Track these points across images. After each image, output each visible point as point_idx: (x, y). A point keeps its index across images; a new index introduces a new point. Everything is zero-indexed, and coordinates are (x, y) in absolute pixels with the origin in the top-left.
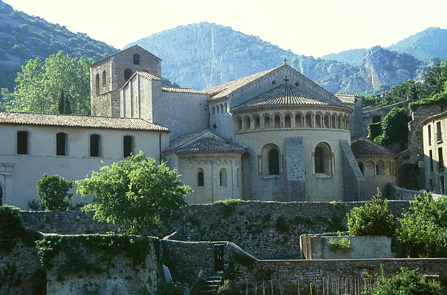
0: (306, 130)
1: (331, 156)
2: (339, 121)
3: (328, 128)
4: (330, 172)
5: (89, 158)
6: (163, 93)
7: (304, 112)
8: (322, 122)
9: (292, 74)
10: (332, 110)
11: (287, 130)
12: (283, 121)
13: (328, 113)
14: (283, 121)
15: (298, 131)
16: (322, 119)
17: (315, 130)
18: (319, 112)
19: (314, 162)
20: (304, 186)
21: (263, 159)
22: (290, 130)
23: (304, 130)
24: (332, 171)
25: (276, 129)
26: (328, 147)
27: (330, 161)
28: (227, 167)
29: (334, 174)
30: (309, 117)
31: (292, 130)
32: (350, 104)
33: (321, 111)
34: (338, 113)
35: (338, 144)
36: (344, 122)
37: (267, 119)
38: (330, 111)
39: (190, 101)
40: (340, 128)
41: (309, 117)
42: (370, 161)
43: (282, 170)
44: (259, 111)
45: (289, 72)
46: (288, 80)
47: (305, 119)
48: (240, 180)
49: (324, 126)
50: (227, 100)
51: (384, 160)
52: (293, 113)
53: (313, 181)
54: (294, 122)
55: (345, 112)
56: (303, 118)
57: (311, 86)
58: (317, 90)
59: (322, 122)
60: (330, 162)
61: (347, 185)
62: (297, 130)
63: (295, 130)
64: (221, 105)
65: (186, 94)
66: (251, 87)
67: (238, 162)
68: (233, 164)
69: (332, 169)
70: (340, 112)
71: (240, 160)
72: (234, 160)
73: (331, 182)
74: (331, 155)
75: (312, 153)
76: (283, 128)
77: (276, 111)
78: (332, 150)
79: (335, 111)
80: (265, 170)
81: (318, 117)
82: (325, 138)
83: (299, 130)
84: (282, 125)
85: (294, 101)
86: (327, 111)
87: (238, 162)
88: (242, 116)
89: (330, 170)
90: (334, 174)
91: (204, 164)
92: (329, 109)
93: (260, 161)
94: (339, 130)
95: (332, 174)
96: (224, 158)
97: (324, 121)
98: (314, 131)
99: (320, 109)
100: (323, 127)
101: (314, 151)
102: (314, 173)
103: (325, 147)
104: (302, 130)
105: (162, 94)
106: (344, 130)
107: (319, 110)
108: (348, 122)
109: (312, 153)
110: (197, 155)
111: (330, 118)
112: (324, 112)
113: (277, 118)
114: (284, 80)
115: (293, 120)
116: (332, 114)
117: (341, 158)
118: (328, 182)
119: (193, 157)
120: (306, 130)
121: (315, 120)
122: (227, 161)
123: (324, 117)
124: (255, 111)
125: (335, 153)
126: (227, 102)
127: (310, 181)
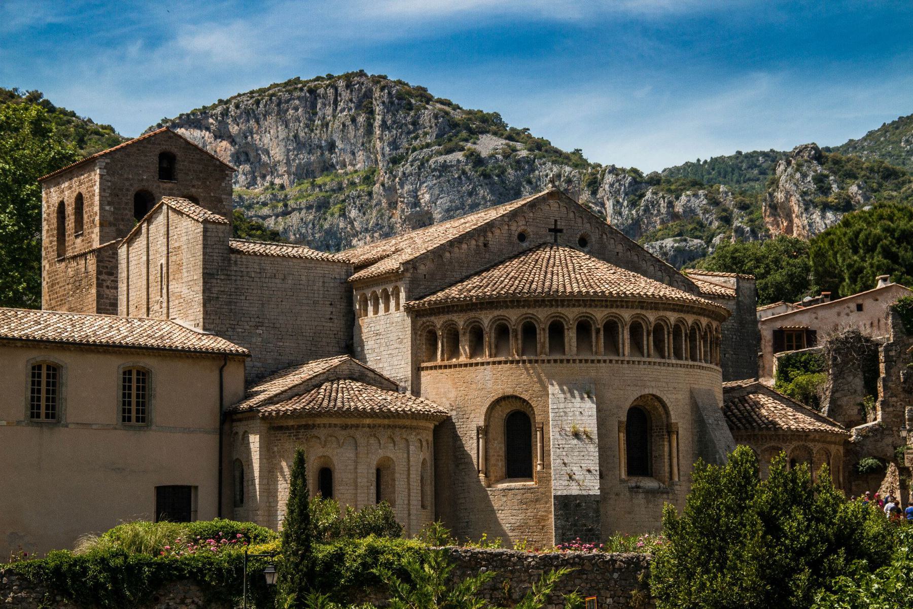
0: (605, 361)
1: (670, 433)
2: (692, 338)
3: (663, 357)
4: (667, 475)
5: (28, 425)
6: (233, 256)
7: (600, 315)
8: (648, 342)
9: (571, 215)
10: (674, 310)
11: (555, 361)
12: (543, 337)
13: (664, 320)
14: (543, 337)
15: (583, 365)
16: (648, 335)
17: (628, 362)
18: (638, 316)
19: (623, 446)
20: (597, 511)
21: (490, 436)
22: (562, 361)
23: (599, 361)
24: (671, 472)
25: (525, 358)
26: (661, 409)
27: (666, 443)
28: (395, 453)
29: (676, 479)
30: (611, 328)
31: (568, 361)
32: (722, 297)
33: (644, 312)
34: (690, 319)
35: (687, 401)
36: (705, 342)
37: (503, 332)
39: (303, 278)
40: (693, 358)
41: (611, 328)
43: (539, 468)
44: (481, 309)
45: (564, 210)
46: (561, 231)
47: (602, 332)
48: (429, 490)
49: (652, 352)
50: (401, 279)
51: (811, 445)
52: (571, 316)
54: (574, 340)
55: (708, 316)
56: (598, 331)
57: (620, 247)
58: (636, 258)
59: (648, 342)
62: (581, 361)
63: (574, 361)
64: (385, 291)
65: (294, 260)
66: (464, 246)
67: (424, 444)
68: (412, 448)
69: (671, 466)
70: (695, 317)
71: (431, 438)
72: (413, 438)
74: (670, 430)
75: (620, 422)
76: (544, 357)
77: (526, 310)
78: (673, 417)
79: (682, 315)
80: (495, 465)
81: (636, 330)
82: (653, 384)
83: (586, 361)
84: (543, 346)
85: (575, 285)
86: (661, 313)
87: (424, 444)
88: (439, 322)
89: (667, 469)
90: (676, 479)
91: (335, 445)
92: (665, 309)
94: (691, 363)
95: (671, 478)
96: (389, 432)
97: (651, 338)
98: (625, 365)
99: (642, 308)
100: (649, 356)
101: (624, 418)
102: (623, 476)
103: (655, 408)
104: (593, 361)
105: (230, 260)
106: (704, 365)
108: (715, 342)
109: (620, 422)
110: (318, 421)
111: (669, 333)
112: (652, 317)
113: (529, 331)
114: (550, 230)
115: (571, 337)
116: (673, 323)
117: (696, 438)
119: (307, 427)
120: (605, 361)
121: (627, 335)
122: (397, 439)
123: (651, 329)
124: (471, 310)
125: (680, 424)
126: (399, 284)
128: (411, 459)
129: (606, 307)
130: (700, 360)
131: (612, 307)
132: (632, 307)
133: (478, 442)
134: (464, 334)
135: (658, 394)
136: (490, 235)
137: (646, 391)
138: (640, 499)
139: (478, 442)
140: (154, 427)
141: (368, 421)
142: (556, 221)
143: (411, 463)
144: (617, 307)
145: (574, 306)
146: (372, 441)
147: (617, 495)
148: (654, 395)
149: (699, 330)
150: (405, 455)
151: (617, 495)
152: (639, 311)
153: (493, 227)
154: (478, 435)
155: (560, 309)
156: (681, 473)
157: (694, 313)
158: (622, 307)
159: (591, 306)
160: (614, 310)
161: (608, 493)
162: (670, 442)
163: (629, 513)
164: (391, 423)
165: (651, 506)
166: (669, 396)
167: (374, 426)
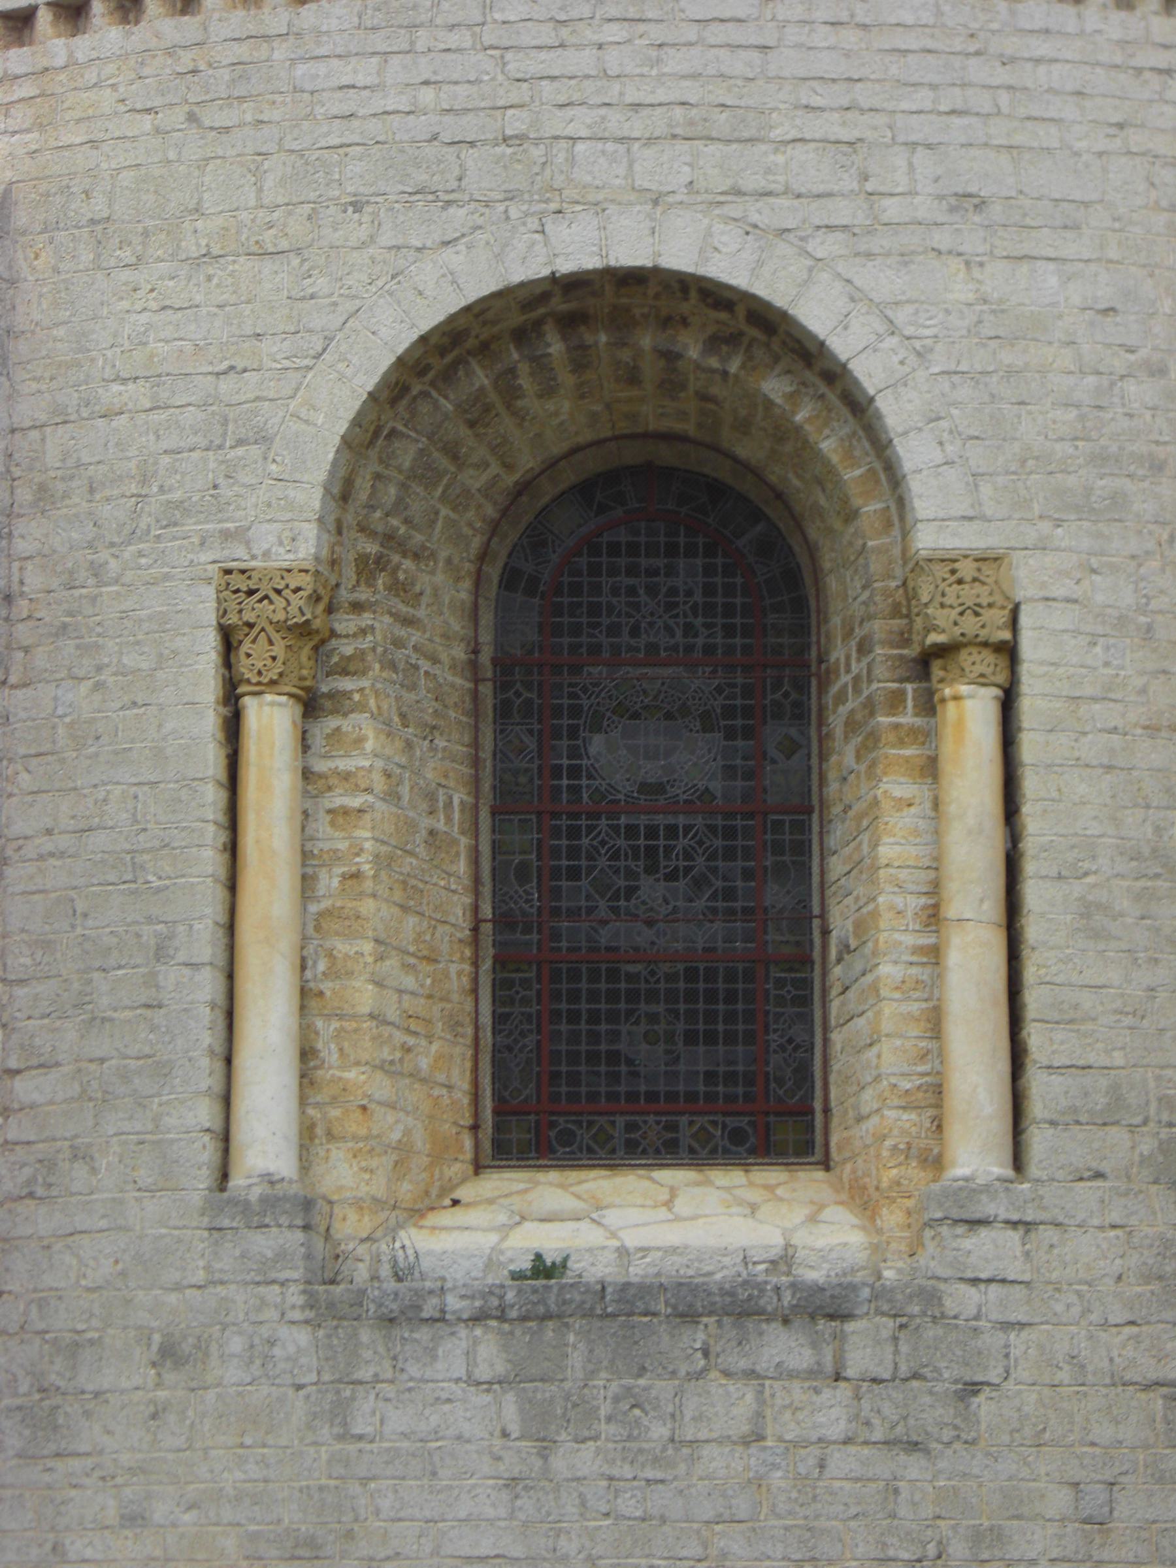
1: (928, 663)
24: (935, 1094)
29: (975, 1154)
60: (896, 846)
69: (935, 1023)
73: (831, 1412)
75: (239, 585)
82: (667, 168)
109: (239, 585)
118: (727, 1405)
125: (1027, 578)
135: (732, 265)
137: (577, 249)
138: (456, 1395)
147: (169, 1354)
156: (1042, 1089)
161: (73, 1349)
162: (931, 769)
165: (578, 1459)
166: (882, 280)
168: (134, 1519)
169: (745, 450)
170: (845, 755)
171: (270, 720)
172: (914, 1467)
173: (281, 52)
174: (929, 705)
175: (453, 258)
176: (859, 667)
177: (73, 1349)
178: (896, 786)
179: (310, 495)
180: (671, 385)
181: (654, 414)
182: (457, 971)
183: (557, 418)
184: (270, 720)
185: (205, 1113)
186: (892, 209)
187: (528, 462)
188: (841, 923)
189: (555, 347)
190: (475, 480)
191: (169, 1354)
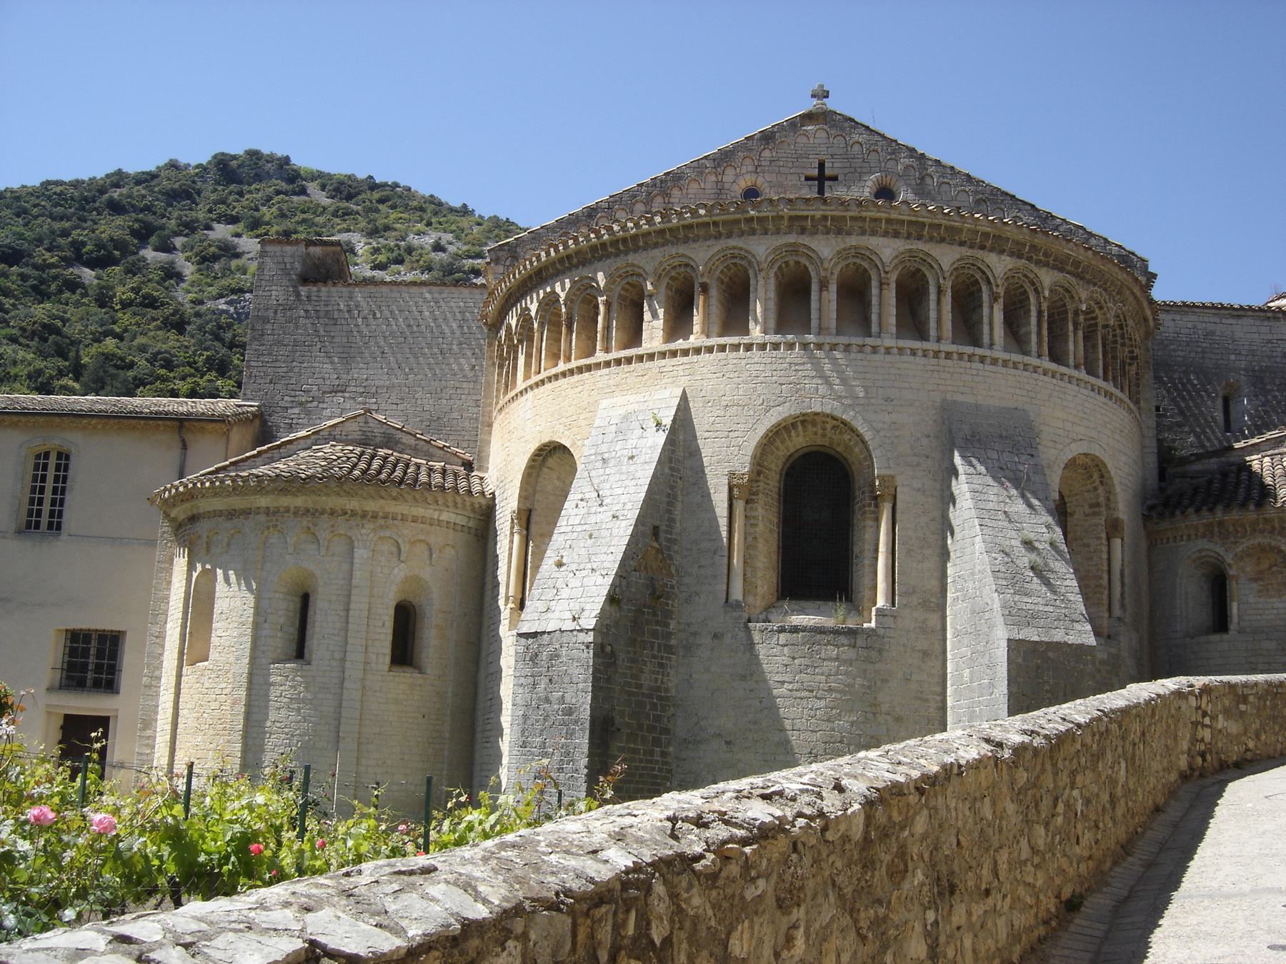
6: (304, 290)
18: (794, 249)
33: (804, 240)
38: (874, 242)
42: (1263, 549)
53: (728, 640)
56: (705, 288)
60: (868, 536)
61: (966, 673)
75: (732, 475)
86: (853, 241)
93: (516, 538)
96: (305, 522)
99: (803, 231)
105: (298, 295)
107: (791, 239)
109: (732, 475)
122: (324, 535)
125: (899, 481)
127: (706, 640)
128: (357, 574)
129: (718, 236)
130: (991, 345)
131: (729, 236)
132: (778, 232)
133: (512, 542)
134: (520, 341)
136: (676, 192)
139: (512, 542)
140: (64, 536)
141: (263, 502)
142: (822, 165)
143: (354, 582)
144: (742, 234)
145: (656, 245)
146: (274, 538)
147: (716, 636)
148: (834, 418)
149: (989, 282)
150: (345, 567)
151: (716, 636)
152: (791, 239)
153: (680, 178)
154: (512, 528)
155: (631, 258)
157: (962, 244)
158: (753, 232)
159: (686, 240)
160: (732, 242)
161: (695, 634)
163: (743, 678)
164: (310, 505)
167: (276, 511)
168: (707, 670)
169: (839, 449)
170: (858, 515)
171: (739, 506)
172: (870, 666)
173: (744, 362)
174: (877, 506)
175: (780, 408)
176: (861, 498)
177: (695, 634)
178: (870, 523)
179: (748, 459)
180: (824, 436)
181: (819, 442)
182: (775, 557)
183: (799, 441)
184: (739, 506)
185: (725, 587)
186: (873, 401)
187: (792, 450)
188: (856, 550)
189: (800, 428)
190: (781, 453)
191: (716, 636)
